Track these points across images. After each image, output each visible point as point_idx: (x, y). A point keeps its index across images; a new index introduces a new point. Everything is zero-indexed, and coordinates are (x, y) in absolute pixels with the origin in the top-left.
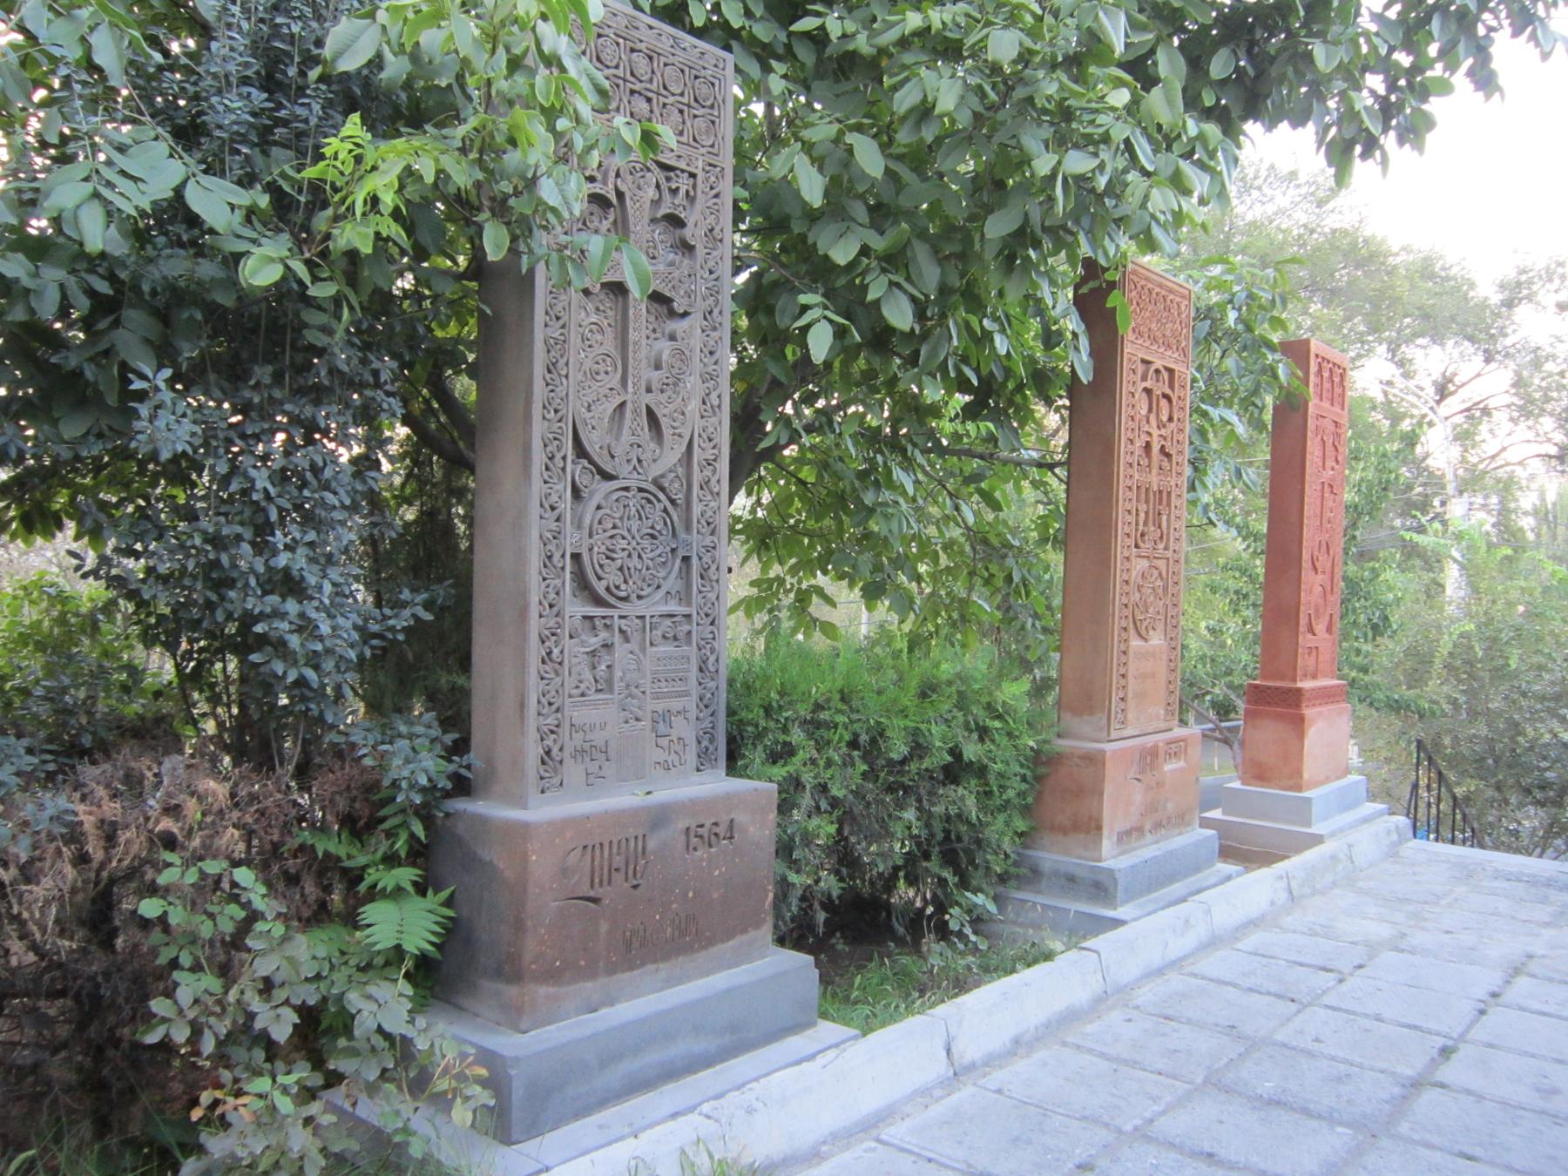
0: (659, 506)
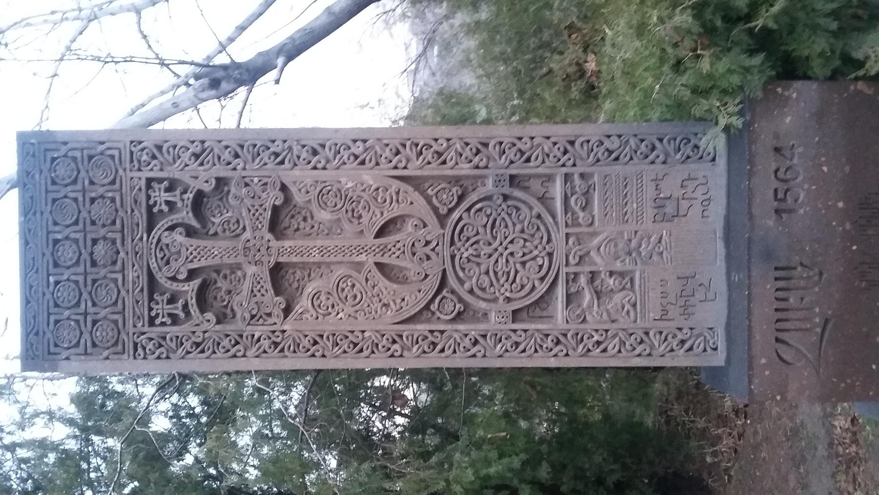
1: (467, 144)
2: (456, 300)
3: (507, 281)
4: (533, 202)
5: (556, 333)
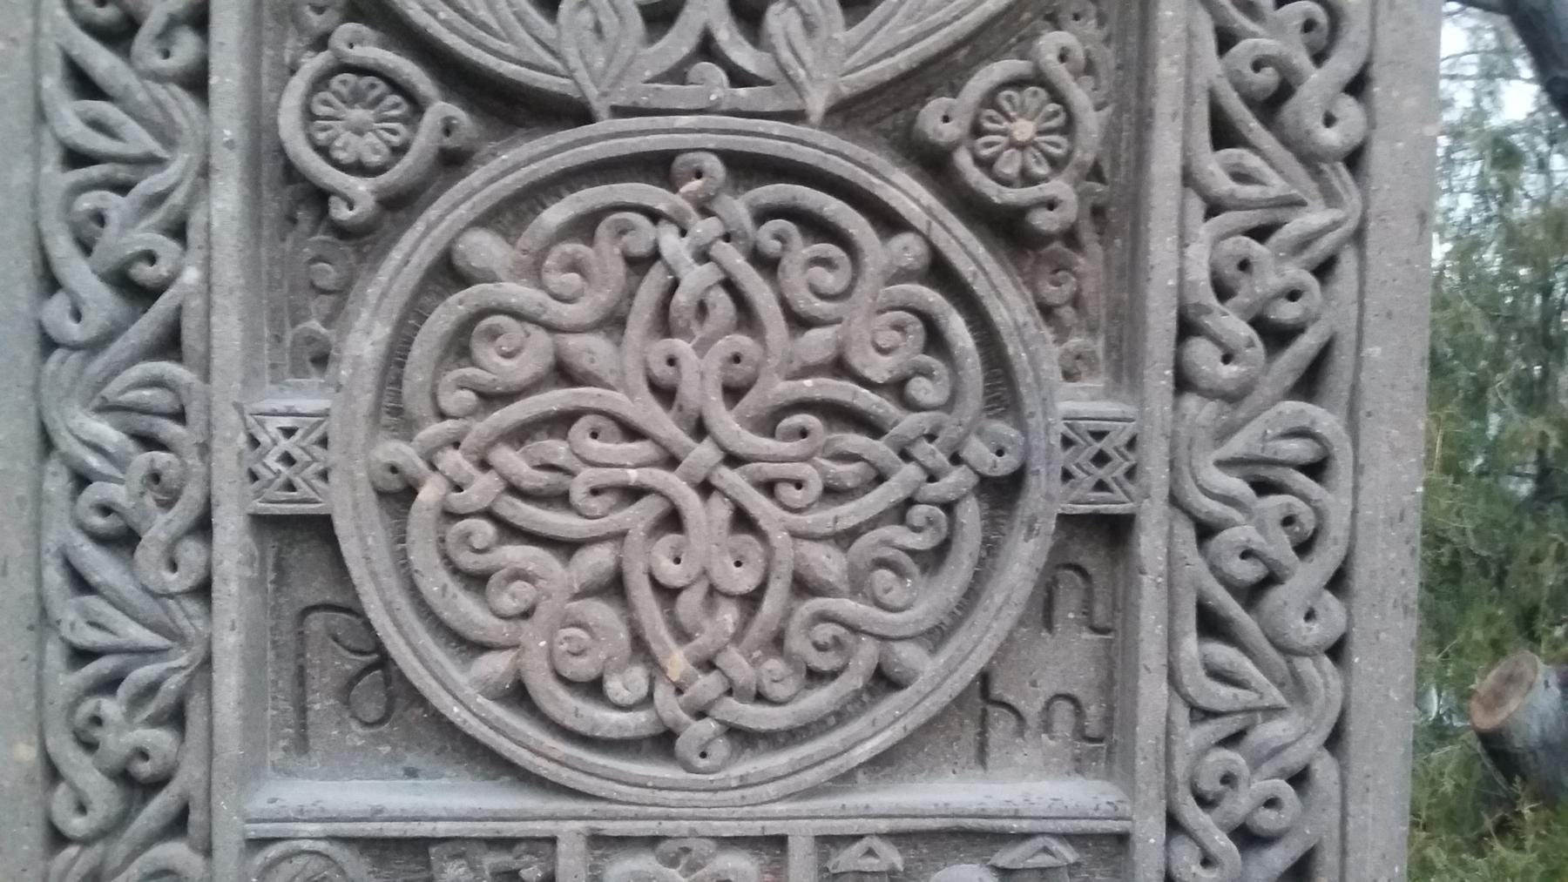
0: (484, 248)
1: (1324, 270)
2: (397, 174)
3: (514, 490)
4: (974, 648)
5: (188, 779)
